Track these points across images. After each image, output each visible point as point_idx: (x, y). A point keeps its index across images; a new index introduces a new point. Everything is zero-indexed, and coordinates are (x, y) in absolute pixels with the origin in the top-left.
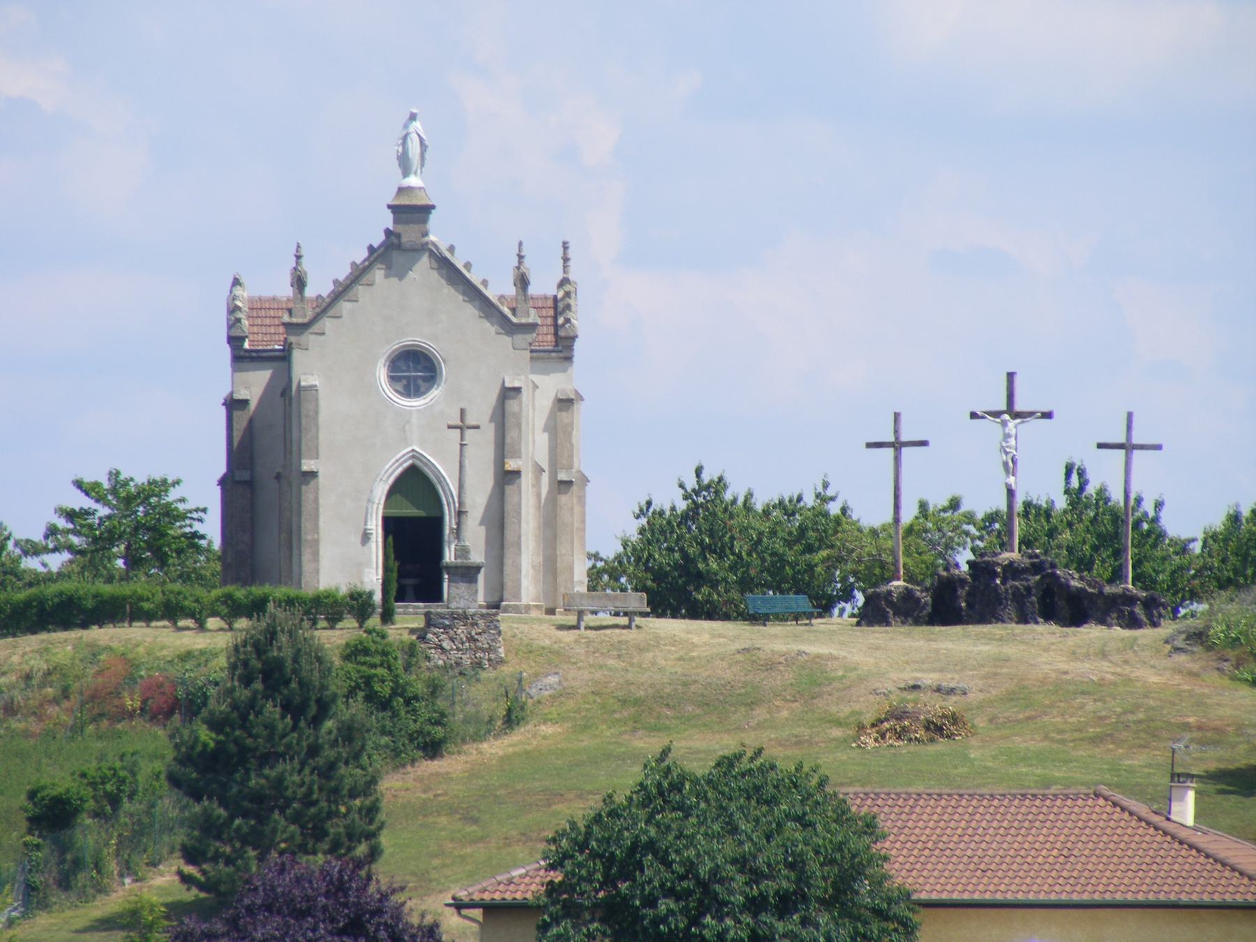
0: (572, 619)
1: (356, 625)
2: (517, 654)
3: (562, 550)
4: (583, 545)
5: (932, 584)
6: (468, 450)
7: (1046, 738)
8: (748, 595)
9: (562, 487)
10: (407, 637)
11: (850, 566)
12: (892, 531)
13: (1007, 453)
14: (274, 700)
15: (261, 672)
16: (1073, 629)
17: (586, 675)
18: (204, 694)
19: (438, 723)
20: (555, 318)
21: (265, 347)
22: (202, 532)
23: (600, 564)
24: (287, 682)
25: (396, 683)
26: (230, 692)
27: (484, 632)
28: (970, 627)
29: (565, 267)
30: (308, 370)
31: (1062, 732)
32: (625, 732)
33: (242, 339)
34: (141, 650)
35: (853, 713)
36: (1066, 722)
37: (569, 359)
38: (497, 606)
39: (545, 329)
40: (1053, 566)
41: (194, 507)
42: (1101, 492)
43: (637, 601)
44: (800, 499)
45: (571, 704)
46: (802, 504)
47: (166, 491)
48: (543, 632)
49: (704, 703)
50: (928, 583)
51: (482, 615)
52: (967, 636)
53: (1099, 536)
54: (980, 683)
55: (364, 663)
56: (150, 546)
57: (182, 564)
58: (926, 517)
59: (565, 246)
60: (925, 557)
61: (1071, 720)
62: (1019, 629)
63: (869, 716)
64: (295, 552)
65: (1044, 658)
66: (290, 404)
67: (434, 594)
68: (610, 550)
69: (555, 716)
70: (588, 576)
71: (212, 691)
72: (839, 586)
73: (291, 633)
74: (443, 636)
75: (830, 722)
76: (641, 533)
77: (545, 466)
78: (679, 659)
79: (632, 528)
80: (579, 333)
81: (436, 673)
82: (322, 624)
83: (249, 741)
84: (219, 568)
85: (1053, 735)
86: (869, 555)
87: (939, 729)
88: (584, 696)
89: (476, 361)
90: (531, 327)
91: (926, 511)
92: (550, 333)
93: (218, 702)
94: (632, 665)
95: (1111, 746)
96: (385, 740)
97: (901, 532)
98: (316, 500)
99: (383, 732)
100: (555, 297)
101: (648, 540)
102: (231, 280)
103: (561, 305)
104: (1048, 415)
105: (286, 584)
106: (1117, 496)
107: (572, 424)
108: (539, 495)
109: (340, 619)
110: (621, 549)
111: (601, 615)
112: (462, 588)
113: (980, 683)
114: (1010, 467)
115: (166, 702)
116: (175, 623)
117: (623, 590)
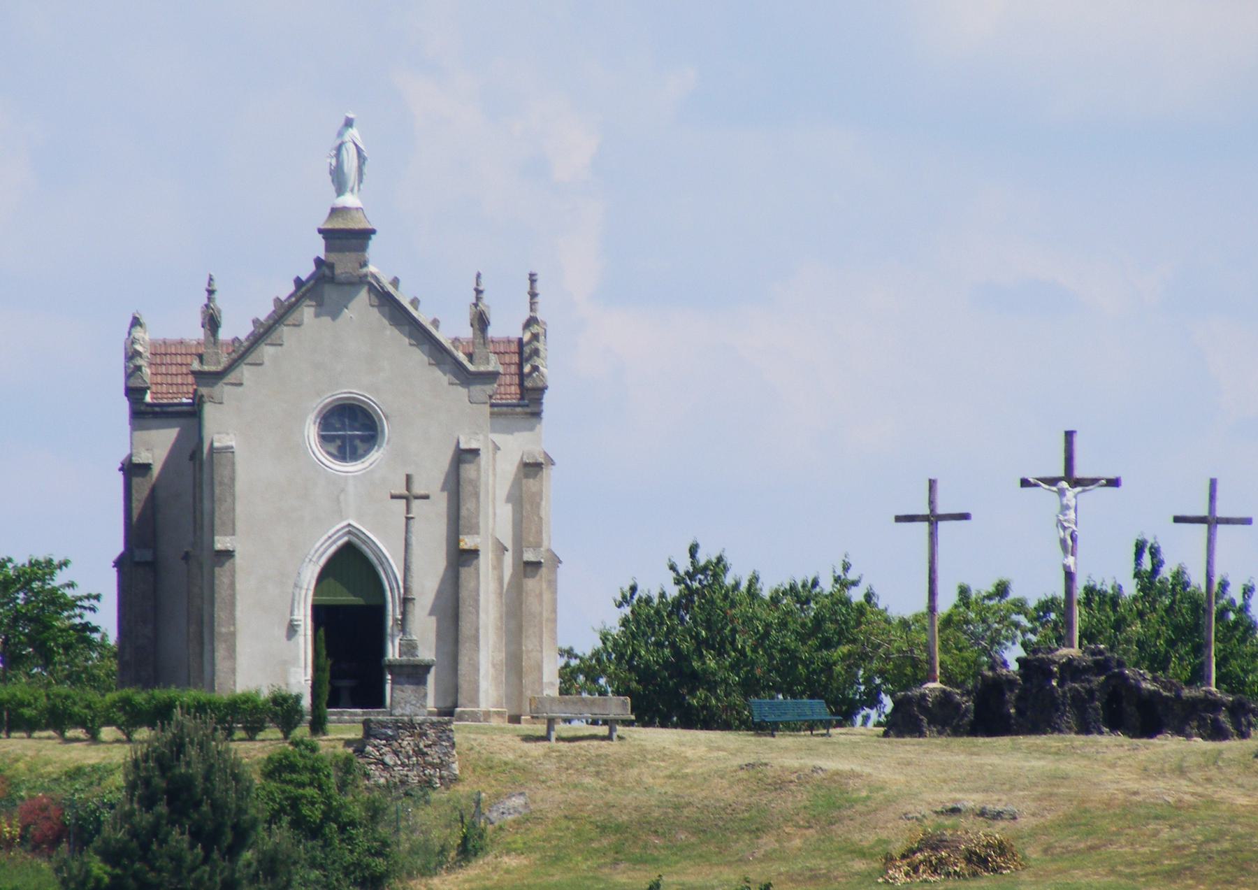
0: (541, 729)
1: (281, 735)
2: (474, 771)
3: (529, 644)
4: (554, 639)
5: (975, 687)
6: (415, 525)
7: (1112, 871)
8: (753, 699)
9: (529, 569)
10: (341, 750)
11: (875, 664)
12: (926, 622)
13: (1065, 528)
14: (181, 826)
15: (167, 792)
16: (1144, 740)
17: (557, 796)
18: (97, 819)
19: (379, 854)
20: (520, 366)
21: (171, 399)
22: (94, 624)
23: (574, 662)
24: (197, 805)
25: (329, 805)
26: (128, 816)
27: (434, 744)
28: (1021, 739)
29: (532, 304)
30: (220, 428)
31: (1131, 864)
32: (605, 865)
33: (143, 391)
34: (21, 765)
35: (880, 842)
36: (1136, 853)
37: (537, 415)
38: (450, 713)
39: (508, 379)
40: (1121, 664)
41: (85, 594)
42: (1179, 575)
43: (618, 706)
44: (815, 583)
45: (539, 831)
46: (818, 589)
47: (52, 574)
48: (505, 744)
49: (699, 829)
50: (970, 684)
51: (433, 724)
52: (1016, 749)
53: (1177, 628)
54: (1033, 806)
55: (290, 782)
56: (31, 641)
57: (71, 662)
58: (967, 605)
59: (532, 279)
60: (967, 654)
61: (1142, 850)
62: (1079, 740)
63: (898, 845)
64: (207, 648)
65: (1111, 775)
66: (201, 469)
67: (374, 699)
68: (587, 645)
69: (520, 845)
70: (560, 676)
71: (107, 815)
72: (862, 688)
73: (201, 745)
74: (385, 749)
75: (852, 852)
76: (623, 625)
77: (508, 544)
78: (670, 777)
79: (613, 619)
80: (549, 384)
81: (376, 794)
82: (240, 734)
83: (151, 876)
84: (114, 668)
85: (1120, 868)
86: (899, 651)
87: (983, 862)
88: (555, 821)
89: (426, 419)
90: (492, 377)
91: (968, 598)
92: (515, 384)
93: (115, 829)
94: (613, 783)
95: (1190, 882)
96: (315, 874)
97: (937, 623)
98: (232, 585)
99: (313, 865)
100: (520, 340)
101: (632, 633)
102: (130, 319)
103: (527, 350)
104: (1114, 483)
105: (195, 687)
106: (1197, 579)
107: (540, 493)
108: (501, 580)
109: (261, 729)
110: (600, 645)
111: (576, 724)
112: (408, 691)
113: (1033, 806)
114: (1069, 545)
115: (51, 828)
116: (62, 734)
117: (603, 693)
